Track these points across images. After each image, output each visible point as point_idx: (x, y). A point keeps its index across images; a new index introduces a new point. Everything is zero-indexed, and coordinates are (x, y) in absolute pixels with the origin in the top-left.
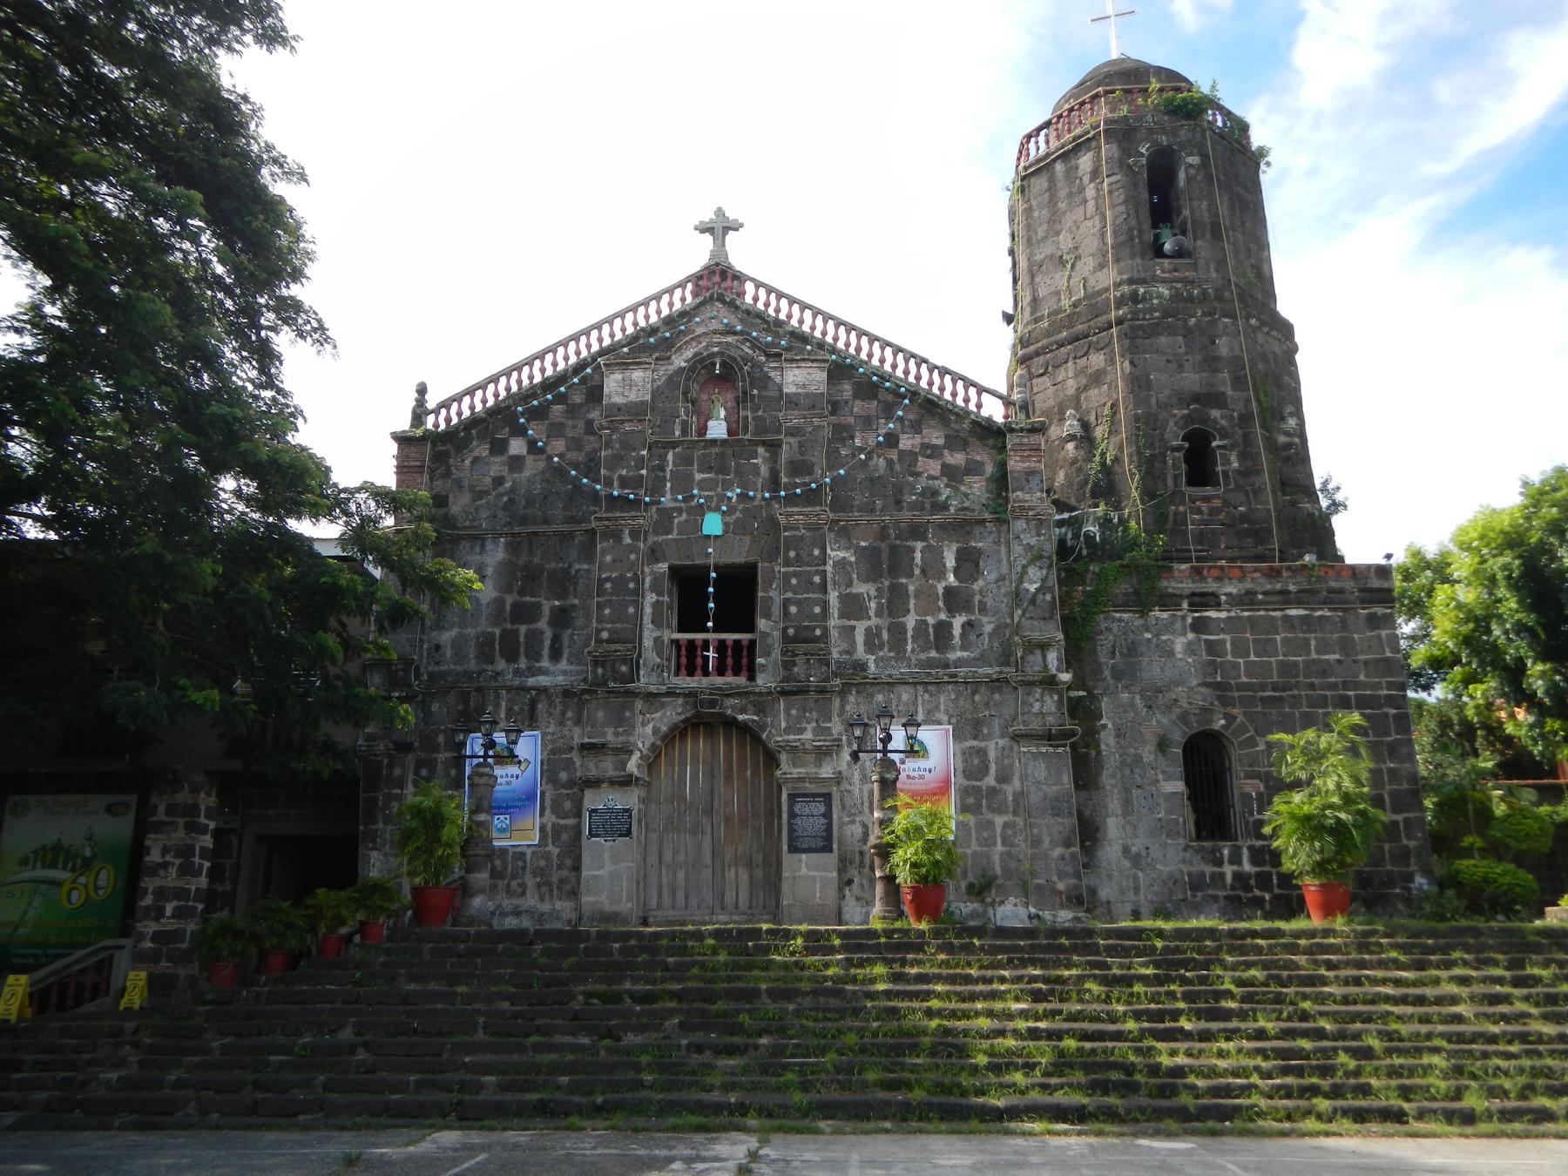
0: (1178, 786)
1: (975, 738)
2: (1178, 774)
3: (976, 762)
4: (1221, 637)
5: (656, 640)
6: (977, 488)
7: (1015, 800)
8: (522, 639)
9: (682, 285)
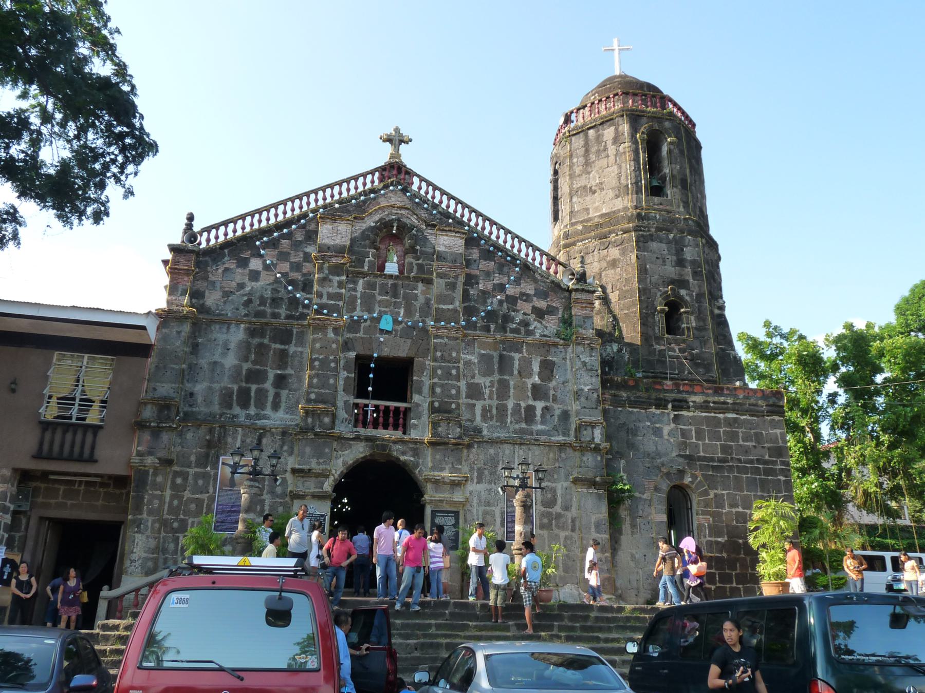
0: (664, 518)
1: (549, 481)
2: (664, 510)
3: (549, 496)
4: (690, 427)
5: (345, 402)
6: (552, 325)
7: (573, 521)
8: (253, 394)
9: (372, 172)
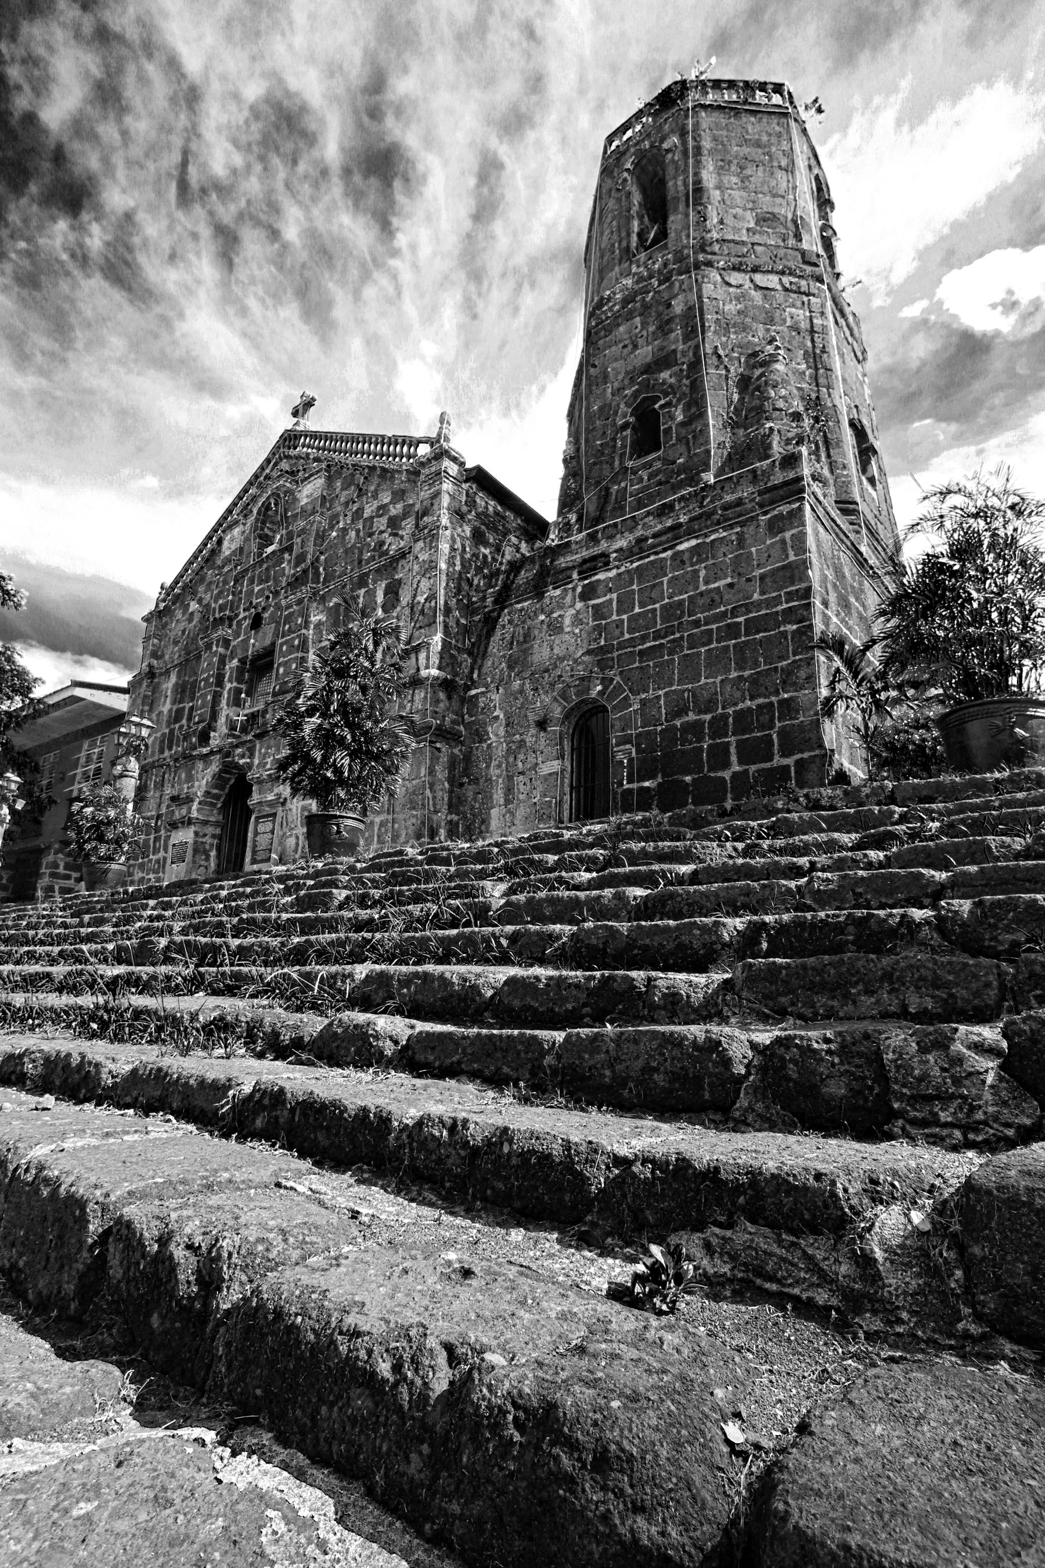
4: (608, 597)
